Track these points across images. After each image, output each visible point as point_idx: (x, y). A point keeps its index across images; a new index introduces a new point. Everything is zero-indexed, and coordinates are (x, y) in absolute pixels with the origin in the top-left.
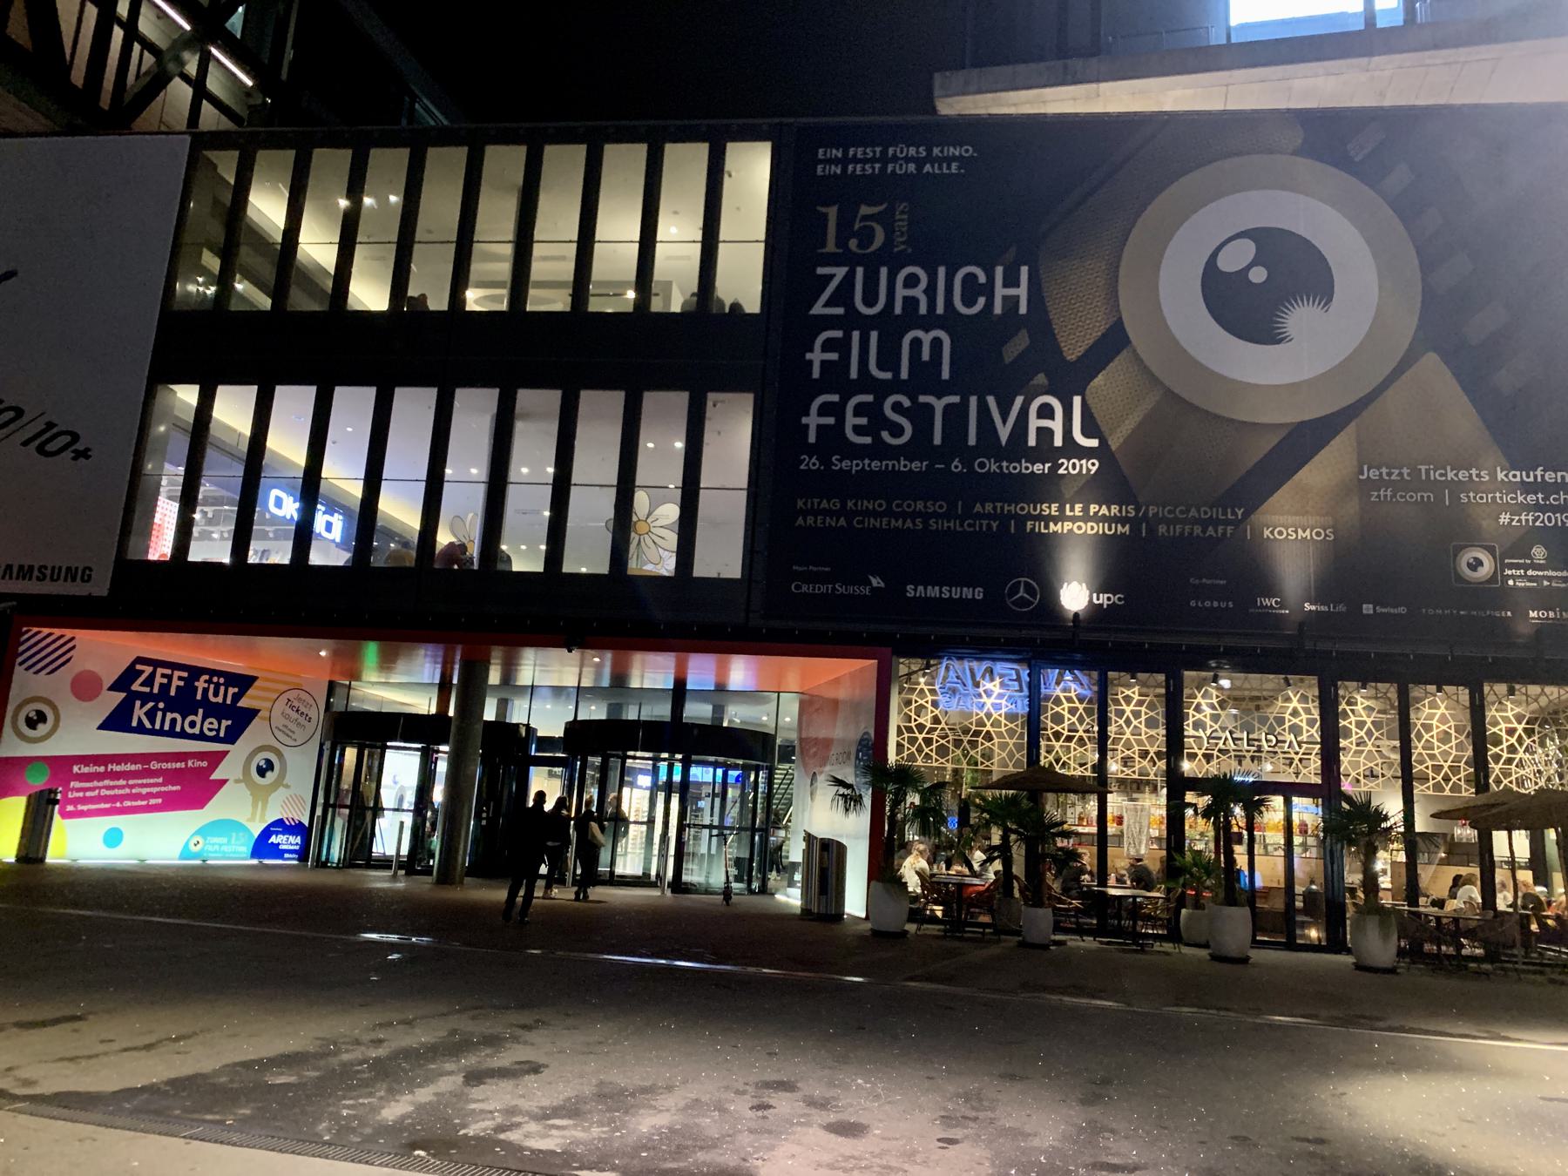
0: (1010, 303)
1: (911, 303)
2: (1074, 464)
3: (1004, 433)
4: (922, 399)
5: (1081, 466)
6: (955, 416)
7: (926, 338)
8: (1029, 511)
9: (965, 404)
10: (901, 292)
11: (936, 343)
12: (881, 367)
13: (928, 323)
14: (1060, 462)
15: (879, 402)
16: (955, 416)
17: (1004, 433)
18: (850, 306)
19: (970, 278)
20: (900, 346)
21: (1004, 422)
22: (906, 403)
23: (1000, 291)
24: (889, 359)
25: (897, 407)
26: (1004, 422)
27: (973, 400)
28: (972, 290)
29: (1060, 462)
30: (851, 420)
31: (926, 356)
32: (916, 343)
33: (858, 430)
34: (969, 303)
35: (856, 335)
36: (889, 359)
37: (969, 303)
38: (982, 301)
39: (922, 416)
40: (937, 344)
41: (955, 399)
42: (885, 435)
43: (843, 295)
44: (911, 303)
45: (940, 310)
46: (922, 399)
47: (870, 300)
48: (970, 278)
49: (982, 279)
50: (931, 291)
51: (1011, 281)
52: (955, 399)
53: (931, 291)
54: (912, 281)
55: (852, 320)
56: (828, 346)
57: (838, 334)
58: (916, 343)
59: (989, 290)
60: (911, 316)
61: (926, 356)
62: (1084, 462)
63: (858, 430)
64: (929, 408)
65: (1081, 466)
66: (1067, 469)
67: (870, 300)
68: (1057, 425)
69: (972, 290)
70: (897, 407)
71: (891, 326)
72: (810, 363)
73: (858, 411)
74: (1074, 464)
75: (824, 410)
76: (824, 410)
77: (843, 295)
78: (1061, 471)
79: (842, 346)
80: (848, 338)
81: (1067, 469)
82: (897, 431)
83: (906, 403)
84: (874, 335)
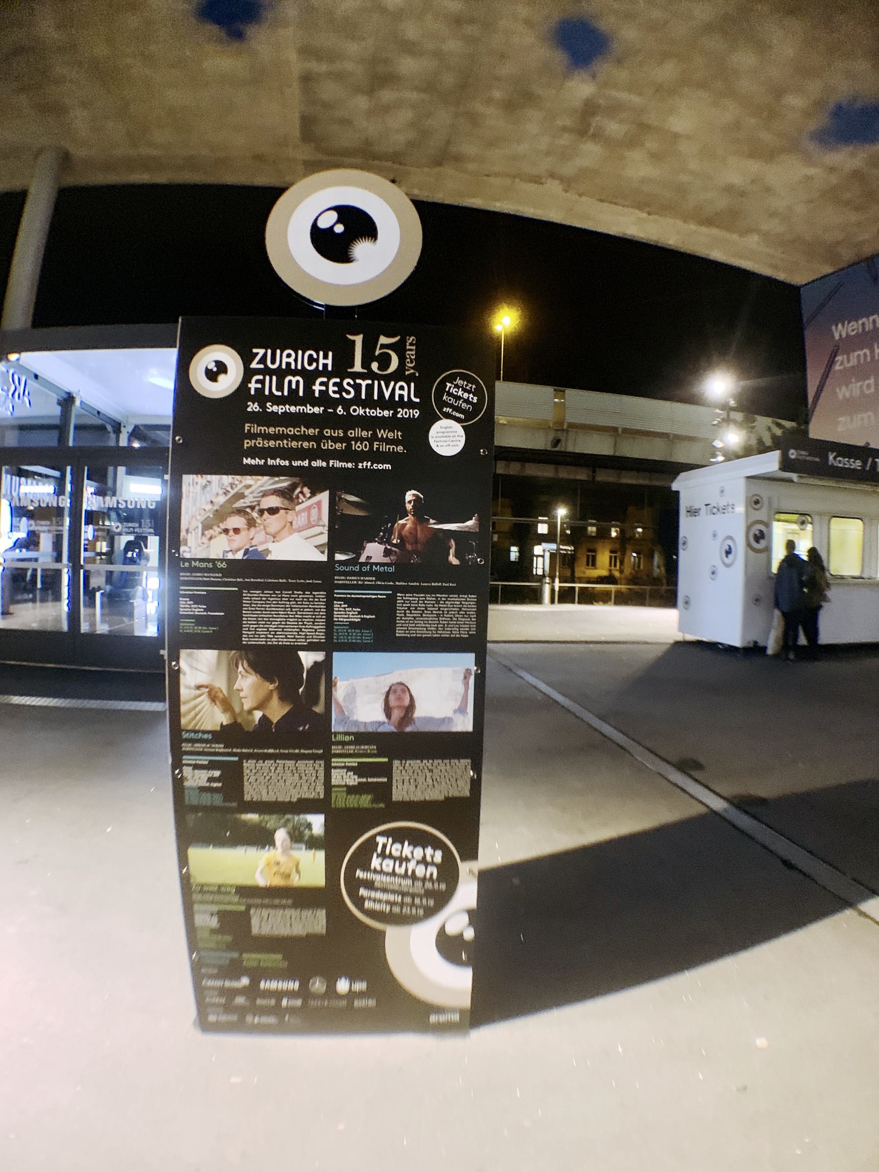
0: (325, 366)
1: (288, 364)
2: (406, 412)
3: (387, 395)
4: (358, 381)
5: (410, 413)
6: (370, 388)
7: (294, 380)
8: (362, 449)
9: (373, 383)
10: (285, 360)
11: (298, 382)
12: (277, 390)
13: (295, 373)
14: (399, 410)
15: (342, 381)
16: (370, 388)
17: (387, 395)
18: (266, 365)
19: (310, 356)
20: (284, 382)
21: (387, 389)
22: (352, 382)
23: (322, 361)
24: (280, 387)
25: (348, 384)
26: (387, 389)
27: (376, 382)
28: (311, 360)
29: (399, 410)
30: (332, 388)
31: (294, 386)
32: (290, 382)
33: (334, 392)
34: (310, 364)
35: (268, 378)
36: (280, 387)
37: (310, 364)
38: (315, 365)
39: (357, 388)
40: (298, 382)
41: (370, 382)
42: (344, 394)
43: (263, 360)
44: (288, 364)
45: (299, 367)
46: (358, 381)
47: (273, 362)
48: (310, 356)
49: (315, 356)
50: (296, 360)
51: (326, 357)
52: (370, 382)
53: (296, 360)
54: (289, 356)
55: (266, 371)
56: (257, 382)
57: (261, 377)
58: (290, 382)
59: (317, 361)
60: (289, 371)
61: (294, 386)
62: (411, 411)
63: (334, 392)
64: (360, 385)
65: (410, 413)
66: (402, 414)
67: (273, 362)
68: (405, 393)
69: (311, 360)
70: (348, 384)
71: (281, 374)
72: (250, 388)
73: (335, 384)
74: (406, 412)
75: (322, 384)
76: (322, 384)
77: (263, 360)
78: (399, 416)
79: (262, 382)
80: (264, 378)
81: (402, 414)
82: (348, 392)
83: (352, 382)
84: (274, 378)
